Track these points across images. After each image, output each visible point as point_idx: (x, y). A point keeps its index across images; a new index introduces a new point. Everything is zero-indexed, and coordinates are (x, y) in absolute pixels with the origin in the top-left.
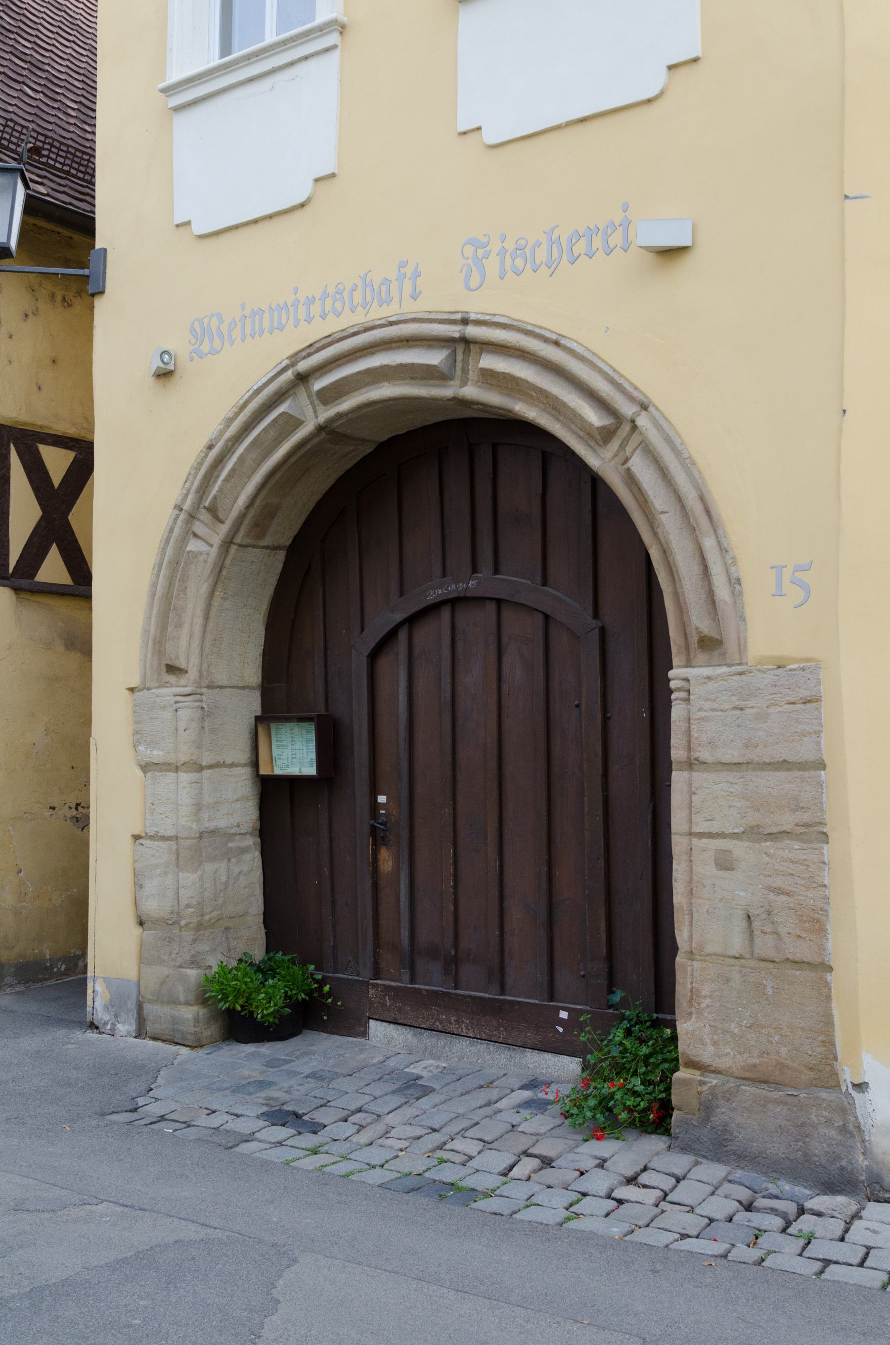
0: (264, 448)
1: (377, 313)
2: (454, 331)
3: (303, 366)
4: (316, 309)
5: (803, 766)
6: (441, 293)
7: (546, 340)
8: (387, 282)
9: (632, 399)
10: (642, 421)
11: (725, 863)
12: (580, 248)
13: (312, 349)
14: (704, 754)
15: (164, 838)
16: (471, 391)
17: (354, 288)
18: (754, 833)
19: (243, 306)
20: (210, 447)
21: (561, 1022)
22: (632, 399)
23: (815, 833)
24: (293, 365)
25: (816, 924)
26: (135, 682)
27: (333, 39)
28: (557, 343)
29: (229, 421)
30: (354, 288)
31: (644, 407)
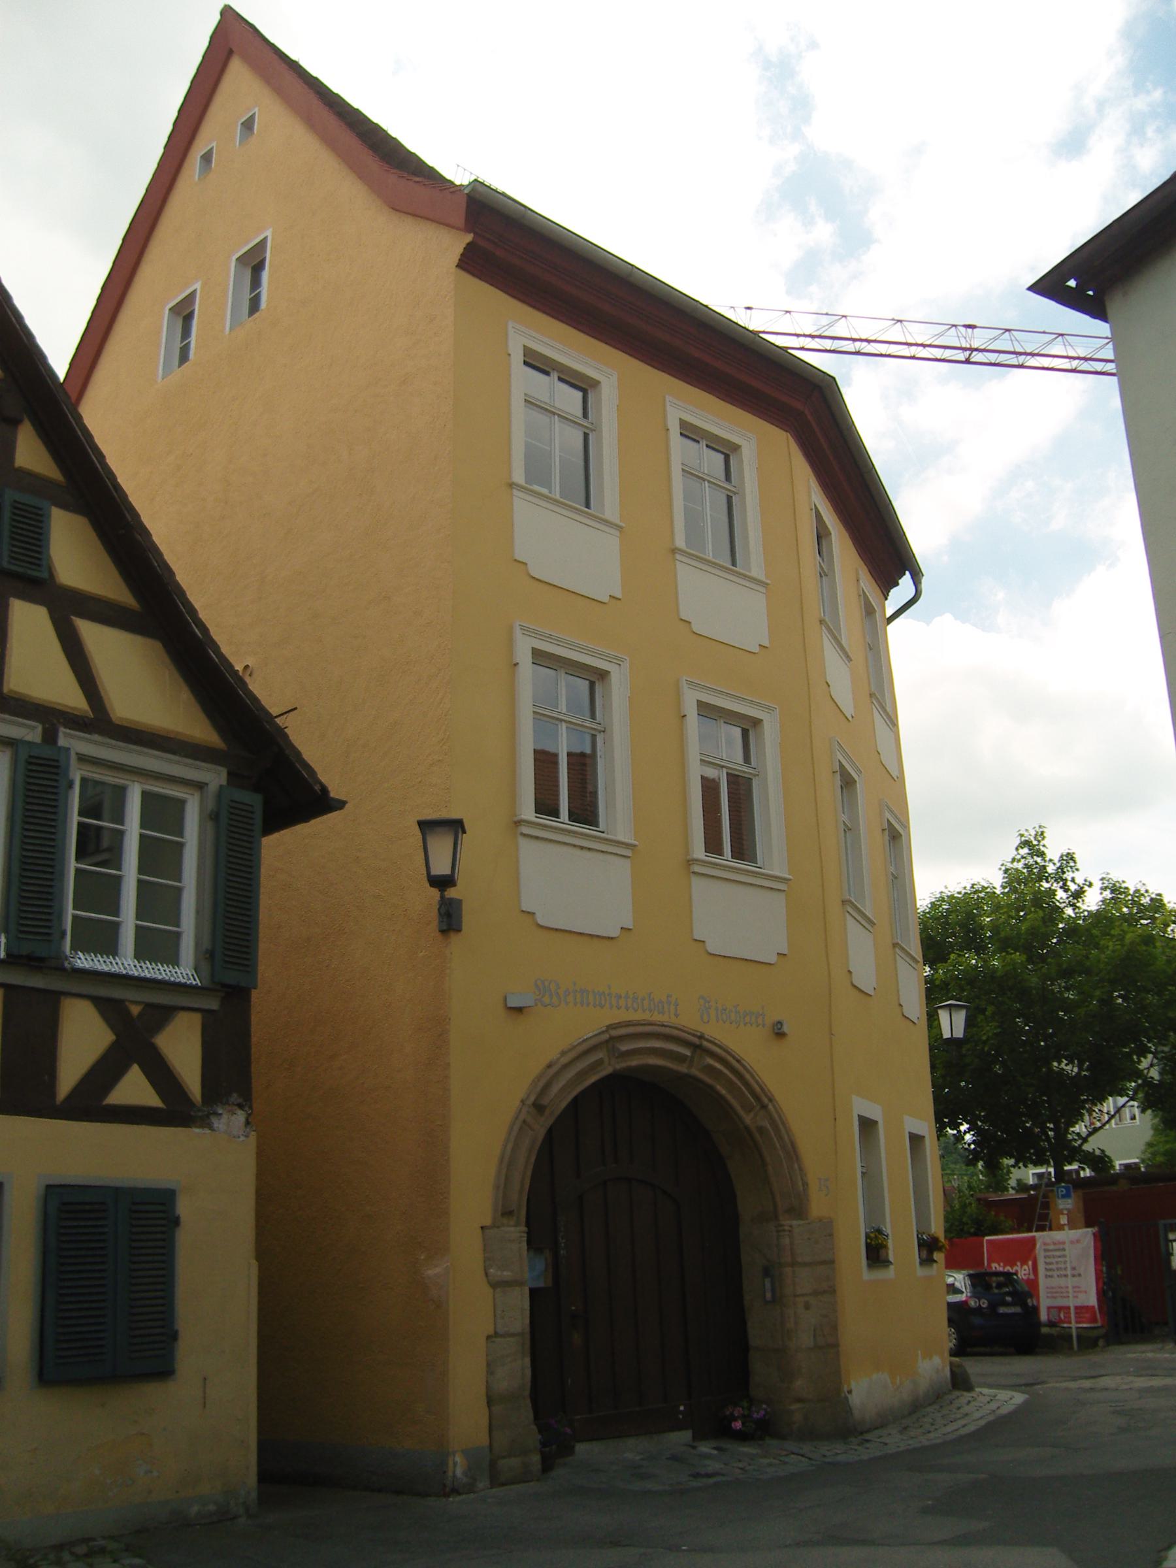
0: (582, 1075)
1: (657, 1018)
2: (696, 1041)
3: (614, 1033)
4: (622, 1002)
5: (824, 1262)
6: (689, 1019)
7: (734, 1057)
8: (661, 1002)
9: (767, 1096)
10: (770, 1106)
11: (807, 1307)
12: (747, 1019)
13: (620, 1025)
14: (799, 1260)
15: (513, 1335)
16: (695, 1072)
17: (643, 999)
18: (816, 1293)
19: (575, 984)
20: (549, 1066)
21: (681, 1412)
22: (767, 1096)
23: (832, 1291)
24: (606, 1031)
25: (834, 1328)
26: (488, 1222)
27: (628, 853)
28: (738, 1061)
29: (563, 1053)
30: (643, 999)
31: (770, 1100)
